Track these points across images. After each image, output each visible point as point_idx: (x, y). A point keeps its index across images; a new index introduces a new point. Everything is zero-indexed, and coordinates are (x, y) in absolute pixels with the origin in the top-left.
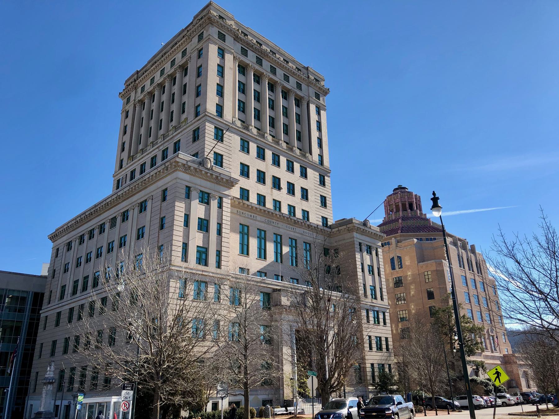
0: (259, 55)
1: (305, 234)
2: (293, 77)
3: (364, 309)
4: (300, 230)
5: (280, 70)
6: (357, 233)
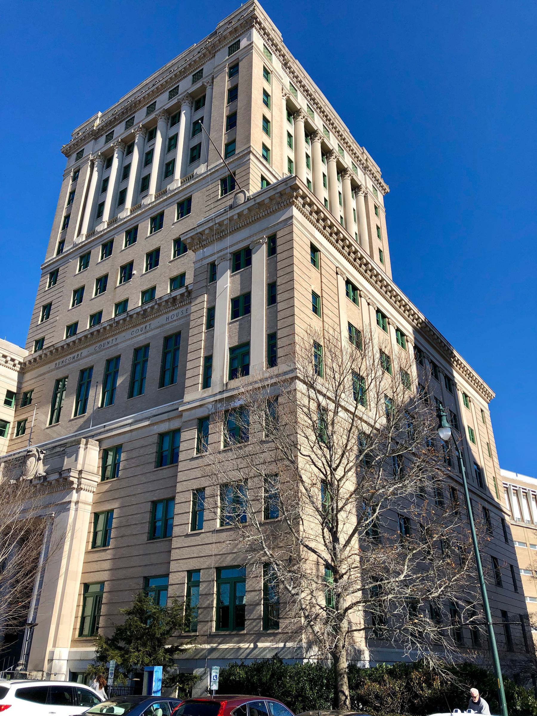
0: (129, 116)
1: (170, 320)
3: (187, 424)
4: (162, 319)
5: (162, 95)
6: (204, 247)
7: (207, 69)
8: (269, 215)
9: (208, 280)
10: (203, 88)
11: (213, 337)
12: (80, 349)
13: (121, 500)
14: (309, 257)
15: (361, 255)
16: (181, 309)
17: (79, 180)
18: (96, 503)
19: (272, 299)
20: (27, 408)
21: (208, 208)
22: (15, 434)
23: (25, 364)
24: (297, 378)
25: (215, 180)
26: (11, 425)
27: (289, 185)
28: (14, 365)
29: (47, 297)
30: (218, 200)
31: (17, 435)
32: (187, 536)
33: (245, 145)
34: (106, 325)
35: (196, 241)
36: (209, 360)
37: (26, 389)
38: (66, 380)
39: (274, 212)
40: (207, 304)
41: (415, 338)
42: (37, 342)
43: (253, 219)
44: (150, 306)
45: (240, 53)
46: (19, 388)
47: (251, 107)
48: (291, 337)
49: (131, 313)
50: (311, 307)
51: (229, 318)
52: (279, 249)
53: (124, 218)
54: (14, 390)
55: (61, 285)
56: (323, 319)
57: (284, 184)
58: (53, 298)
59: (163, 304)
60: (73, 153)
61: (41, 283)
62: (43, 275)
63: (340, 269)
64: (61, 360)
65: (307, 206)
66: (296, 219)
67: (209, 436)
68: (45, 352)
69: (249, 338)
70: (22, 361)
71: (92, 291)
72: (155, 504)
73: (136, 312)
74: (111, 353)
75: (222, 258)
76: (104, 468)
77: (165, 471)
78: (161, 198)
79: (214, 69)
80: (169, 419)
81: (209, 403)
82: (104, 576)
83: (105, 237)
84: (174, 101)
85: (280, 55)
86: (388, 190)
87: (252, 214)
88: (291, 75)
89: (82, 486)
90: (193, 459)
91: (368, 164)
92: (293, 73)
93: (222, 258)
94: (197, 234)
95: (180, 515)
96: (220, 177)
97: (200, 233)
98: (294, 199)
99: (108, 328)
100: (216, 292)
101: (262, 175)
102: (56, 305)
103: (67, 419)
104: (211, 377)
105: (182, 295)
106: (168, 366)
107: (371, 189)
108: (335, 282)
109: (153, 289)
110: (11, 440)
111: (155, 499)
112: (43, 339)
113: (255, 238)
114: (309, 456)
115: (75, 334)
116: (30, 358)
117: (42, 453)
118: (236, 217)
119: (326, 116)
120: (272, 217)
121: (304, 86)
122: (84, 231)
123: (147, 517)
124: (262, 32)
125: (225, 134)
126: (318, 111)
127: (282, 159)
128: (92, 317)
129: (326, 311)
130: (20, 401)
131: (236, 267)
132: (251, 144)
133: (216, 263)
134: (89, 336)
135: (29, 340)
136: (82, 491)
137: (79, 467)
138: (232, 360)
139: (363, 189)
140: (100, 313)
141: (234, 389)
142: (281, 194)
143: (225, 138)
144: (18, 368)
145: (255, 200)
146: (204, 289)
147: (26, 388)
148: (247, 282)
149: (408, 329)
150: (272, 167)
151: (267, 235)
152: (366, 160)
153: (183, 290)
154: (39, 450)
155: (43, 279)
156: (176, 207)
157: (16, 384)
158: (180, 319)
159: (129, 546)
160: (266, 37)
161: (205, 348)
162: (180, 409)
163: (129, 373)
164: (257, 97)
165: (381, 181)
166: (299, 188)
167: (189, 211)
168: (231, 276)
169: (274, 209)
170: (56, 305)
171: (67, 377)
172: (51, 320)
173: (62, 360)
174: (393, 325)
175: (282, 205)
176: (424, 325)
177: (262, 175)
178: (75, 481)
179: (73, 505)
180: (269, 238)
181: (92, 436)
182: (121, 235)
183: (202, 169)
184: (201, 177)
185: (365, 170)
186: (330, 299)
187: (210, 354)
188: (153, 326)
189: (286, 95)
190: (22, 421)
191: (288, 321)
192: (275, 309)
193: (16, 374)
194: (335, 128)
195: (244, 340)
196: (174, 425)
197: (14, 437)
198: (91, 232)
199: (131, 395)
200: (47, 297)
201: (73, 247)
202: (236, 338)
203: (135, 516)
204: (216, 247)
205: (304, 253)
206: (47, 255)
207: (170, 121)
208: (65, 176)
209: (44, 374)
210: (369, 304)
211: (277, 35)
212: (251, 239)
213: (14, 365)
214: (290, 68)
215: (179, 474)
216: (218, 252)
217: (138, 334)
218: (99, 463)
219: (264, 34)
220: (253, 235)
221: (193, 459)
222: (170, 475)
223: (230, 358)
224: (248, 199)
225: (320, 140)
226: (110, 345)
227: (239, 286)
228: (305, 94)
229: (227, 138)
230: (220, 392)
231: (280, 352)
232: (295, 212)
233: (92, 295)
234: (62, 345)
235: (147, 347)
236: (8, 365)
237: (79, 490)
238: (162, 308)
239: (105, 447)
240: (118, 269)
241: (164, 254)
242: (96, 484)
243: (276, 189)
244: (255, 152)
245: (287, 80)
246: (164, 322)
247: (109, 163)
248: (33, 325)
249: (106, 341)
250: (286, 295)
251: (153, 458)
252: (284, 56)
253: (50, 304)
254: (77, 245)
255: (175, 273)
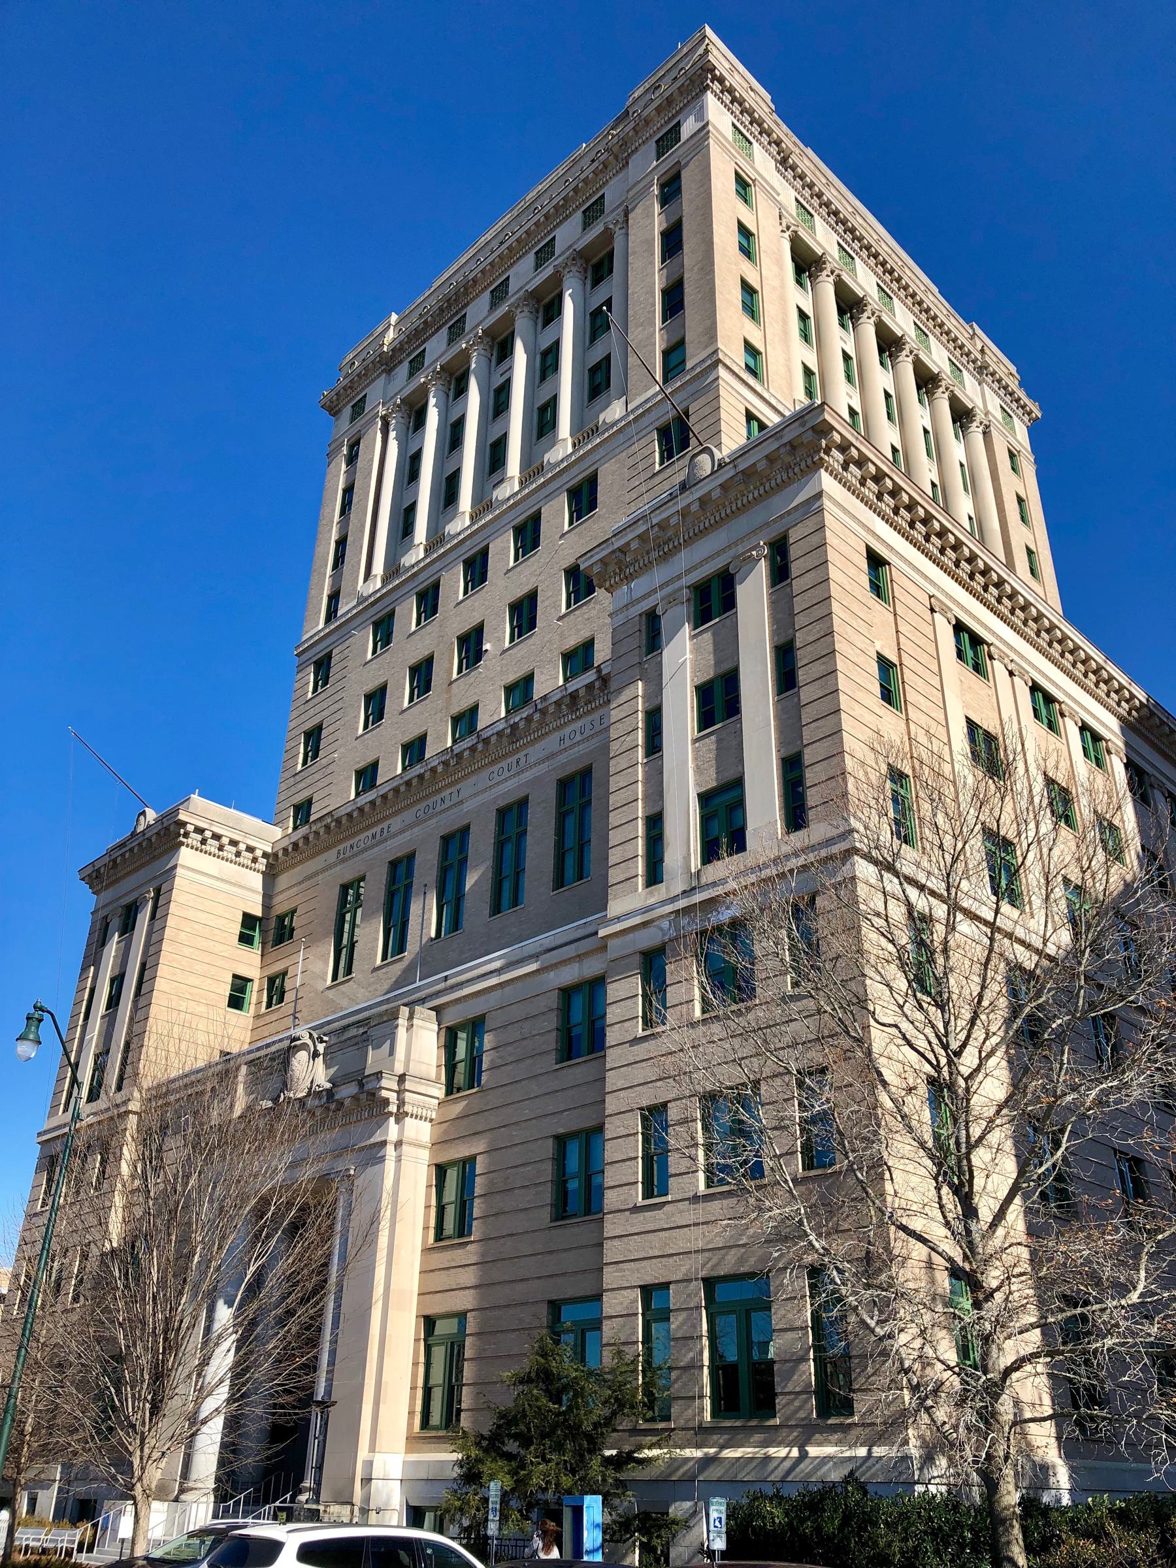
1: (568, 743)
2: (567, 217)
3: (618, 966)
4: (551, 743)
6: (629, 578)
7: (612, 193)
8: (768, 494)
9: (644, 649)
10: (607, 236)
11: (661, 773)
12: (385, 818)
13: (488, 1134)
14: (865, 580)
15: (985, 563)
16: (590, 718)
17: (361, 462)
18: (438, 1144)
19: (786, 679)
20: (286, 947)
21: (634, 495)
22: (264, 1004)
23: (275, 855)
24: (856, 851)
25: (644, 432)
26: (256, 985)
27: (809, 425)
28: (255, 860)
29: (312, 712)
30: (655, 475)
31: (269, 1005)
32: (636, 1209)
33: (706, 347)
34: (436, 763)
35: (612, 567)
36: (655, 822)
37: (280, 908)
38: (362, 884)
39: (781, 487)
40: (644, 703)
41: (1127, 744)
42: (298, 808)
43: (734, 508)
44: (524, 715)
45: (680, 152)
46: (267, 906)
47: (713, 265)
48: (835, 760)
49: (485, 735)
50: (877, 690)
51: (693, 728)
52: (795, 569)
53: (459, 534)
54: (257, 911)
55: (339, 686)
56: (907, 714)
57: (797, 424)
58: (323, 713)
59: (552, 709)
60: (345, 406)
61: (297, 685)
62: (301, 668)
63: (937, 599)
64: (348, 844)
65: (852, 467)
66: (830, 498)
67: (668, 989)
68: (314, 828)
69: (740, 768)
70: (269, 850)
71: (401, 694)
72: (561, 1141)
73: (495, 731)
74: (449, 822)
75: (671, 600)
76: (451, 1067)
77: (578, 1070)
78: (531, 483)
79: (628, 191)
80: (578, 956)
81: (662, 916)
82: (464, 1301)
83: (421, 577)
84: (548, 271)
85: (770, 143)
86: (1037, 413)
87: (732, 494)
88: (798, 183)
89: (408, 1108)
90: (636, 1041)
91: (987, 359)
92: (802, 177)
93: (671, 600)
94: (613, 552)
95: (617, 1165)
96: (657, 424)
97: (619, 549)
98: (822, 455)
99: (440, 769)
100: (661, 675)
101: (747, 410)
102: (331, 730)
103: (368, 967)
104: (662, 860)
105: (590, 687)
106: (570, 841)
107: (999, 414)
108: (929, 630)
109: (528, 679)
110: (257, 1017)
111: (561, 1131)
112: (309, 802)
113: (740, 549)
114: (896, 1026)
115: (373, 785)
116: (285, 843)
117: (322, 1041)
118: (695, 507)
119: (883, 264)
120: (776, 500)
121: (828, 204)
122: (378, 568)
123: (548, 1169)
124: (727, 98)
125: (661, 330)
126: (864, 253)
127: (789, 370)
128: (407, 748)
129: (911, 696)
130: (271, 936)
131: (702, 617)
132: (720, 345)
133: (659, 612)
134: (403, 789)
135: (282, 806)
136: (407, 1119)
137: (399, 1069)
138: (706, 821)
139: (980, 416)
140: (422, 740)
141: (714, 884)
142: (793, 446)
143: (661, 336)
144: (262, 864)
145: (735, 467)
146: (637, 670)
147: (281, 905)
148: (727, 646)
149: (1109, 725)
150: (768, 390)
151: (766, 540)
152: (982, 351)
153: (590, 676)
154: (316, 1036)
155: (300, 676)
156: (564, 498)
157: (259, 899)
158: (587, 739)
159: (512, 1235)
160: (736, 108)
161: (646, 797)
162: (602, 933)
163: (489, 863)
164: (725, 239)
165: (1020, 393)
166: (832, 428)
167: (593, 505)
168: (692, 637)
169: (779, 481)
170: (331, 730)
171: (363, 879)
172: (322, 760)
173: (351, 842)
174: (1072, 717)
175: (797, 470)
176: (1145, 711)
177: (747, 410)
178: (393, 1097)
179: (390, 1150)
180: (771, 545)
181: (422, 1001)
182: (455, 570)
183: (615, 411)
184: (615, 429)
185: (980, 373)
186: (919, 669)
187: (659, 809)
188: (532, 760)
189: (788, 228)
190: (277, 977)
191: (826, 726)
192: (796, 700)
193: (259, 878)
194: (906, 288)
195: (730, 775)
196: (591, 968)
197: (263, 1010)
198: (393, 569)
199: (496, 909)
200: (312, 712)
201: (358, 604)
202: (712, 772)
203: (522, 1169)
204: (658, 575)
205: (852, 571)
206: (307, 625)
207: (541, 314)
208: (331, 455)
209: (316, 874)
210: (1011, 674)
211: (760, 100)
212: (732, 553)
213: (255, 860)
214: (793, 168)
215: (608, 1074)
216: (661, 587)
217: (503, 777)
218: (438, 1058)
219: (732, 102)
220: (736, 543)
221: (636, 1041)
222: (591, 1078)
223: (702, 817)
224: (720, 465)
225: (873, 319)
226: (448, 803)
227: (712, 657)
228: (832, 219)
229: (665, 337)
230: (684, 892)
231: (813, 797)
232: (827, 482)
233: (402, 702)
234: (349, 810)
235: (523, 803)
236: (241, 860)
237: (400, 1116)
238: (548, 718)
239: (450, 1019)
240: (452, 643)
241: (547, 603)
242: (436, 1101)
243: (781, 437)
244: (728, 362)
245: (788, 195)
246: (556, 747)
247: (418, 419)
248: (287, 774)
249: (438, 798)
250: (818, 669)
251: (551, 1041)
252: (778, 143)
253: (319, 728)
254: (367, 598)
255: (572, 641)
